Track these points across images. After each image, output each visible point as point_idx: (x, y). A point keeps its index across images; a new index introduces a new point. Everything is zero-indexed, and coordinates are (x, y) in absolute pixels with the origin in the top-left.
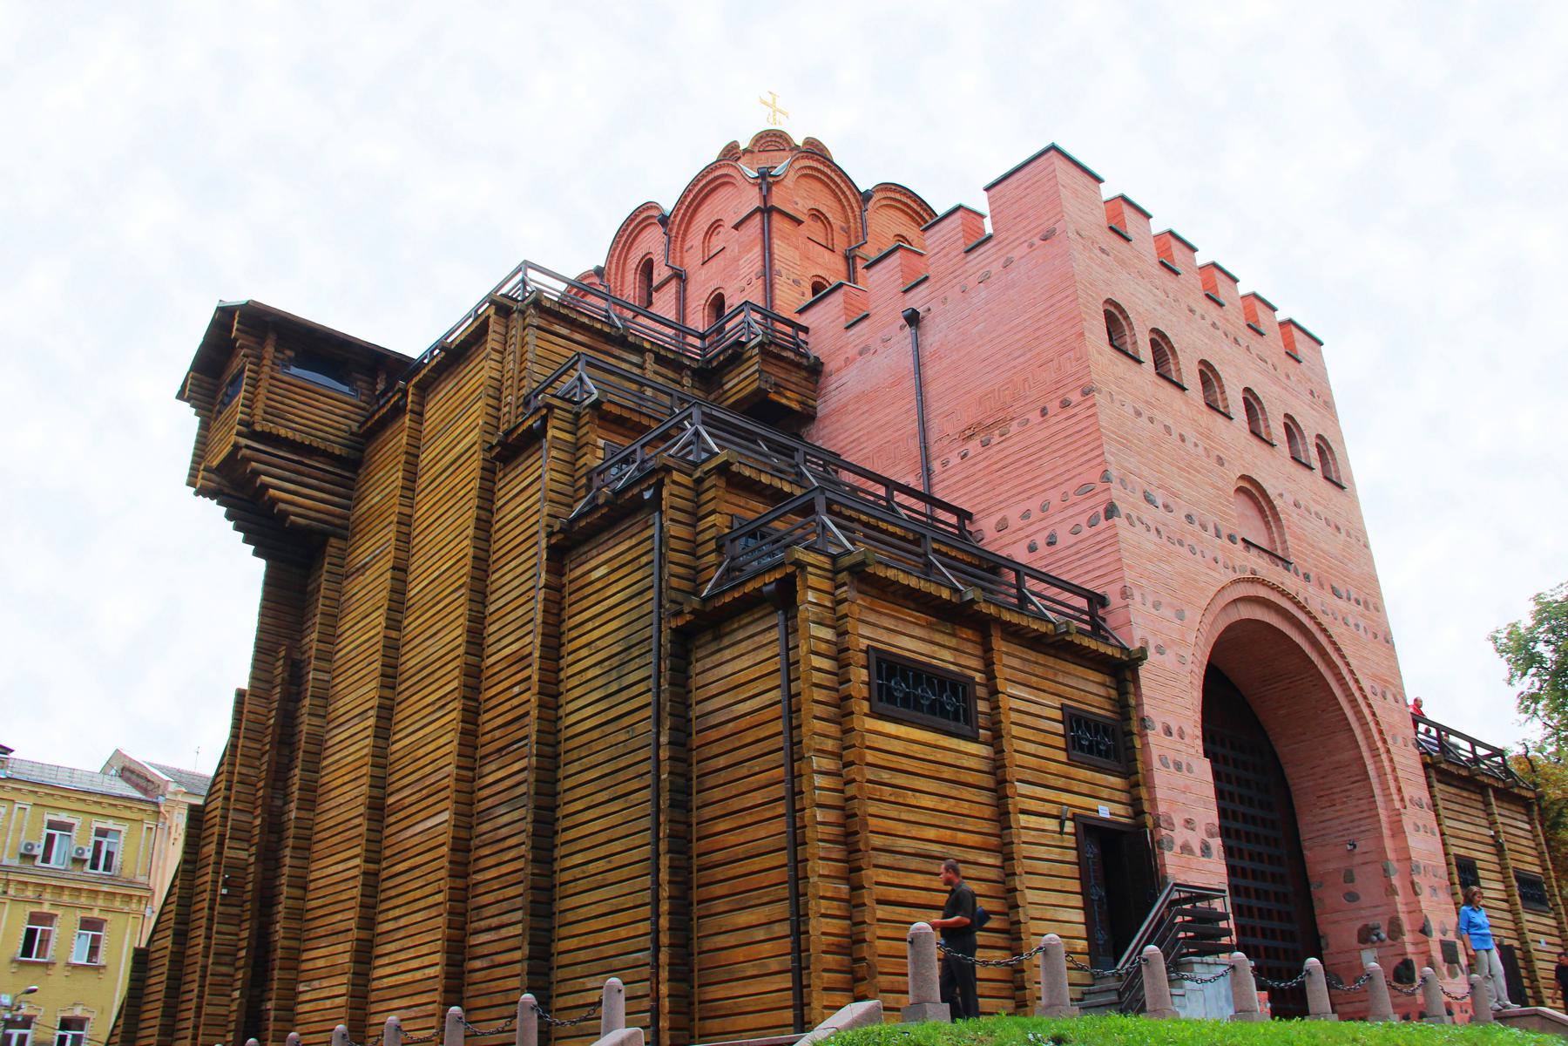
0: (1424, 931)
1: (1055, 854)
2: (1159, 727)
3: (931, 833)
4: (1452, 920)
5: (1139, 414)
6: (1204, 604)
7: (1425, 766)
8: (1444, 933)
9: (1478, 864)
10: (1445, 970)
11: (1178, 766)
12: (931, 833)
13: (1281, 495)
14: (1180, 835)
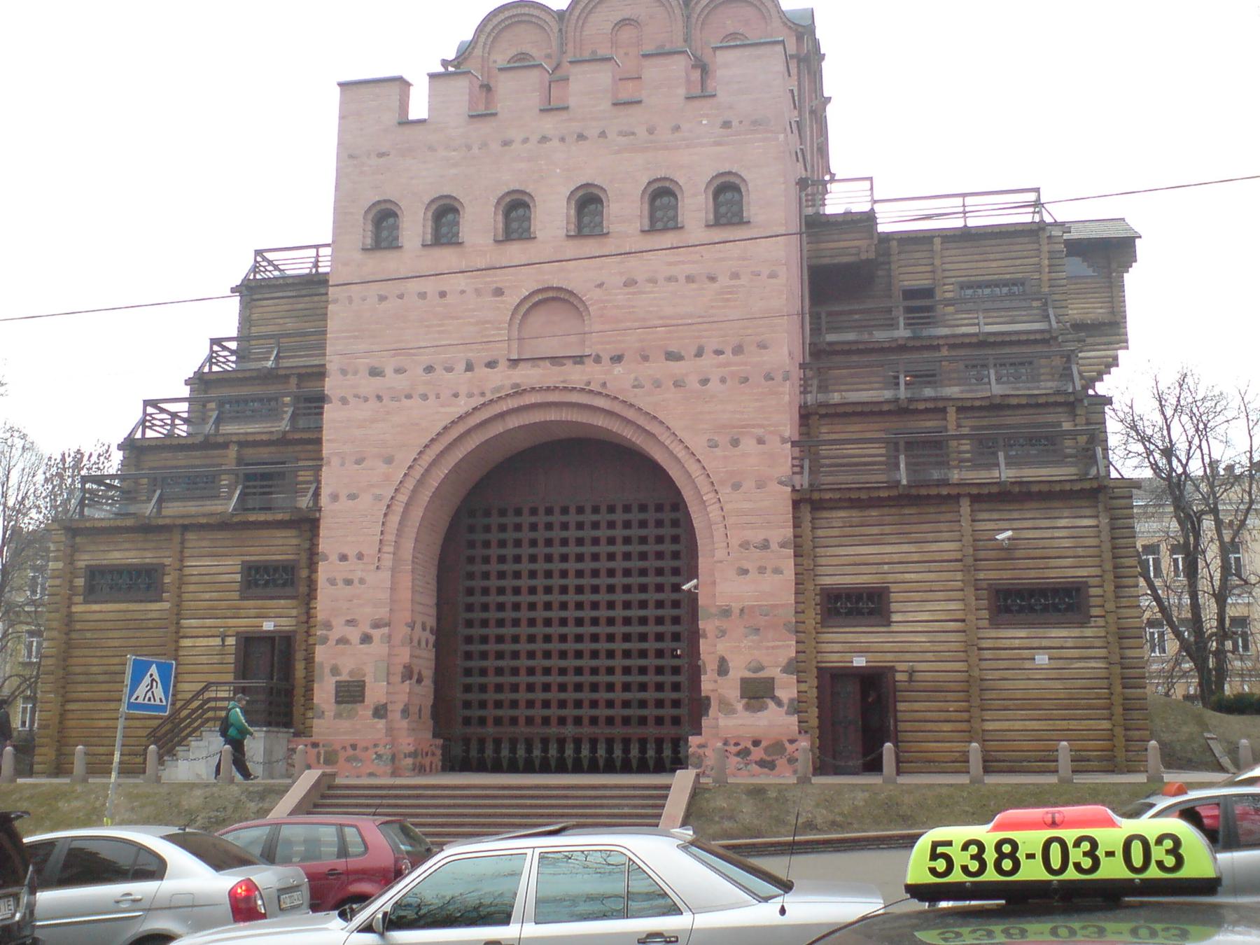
0: (723, 669)
1: (216, 659)
2: (334, 558)
6: (426, 441)
7: (796, 504)
8: (761, 668)
9: (893, 587)
11: (349, 582)
13: (600, 285)
14: (339, 630)
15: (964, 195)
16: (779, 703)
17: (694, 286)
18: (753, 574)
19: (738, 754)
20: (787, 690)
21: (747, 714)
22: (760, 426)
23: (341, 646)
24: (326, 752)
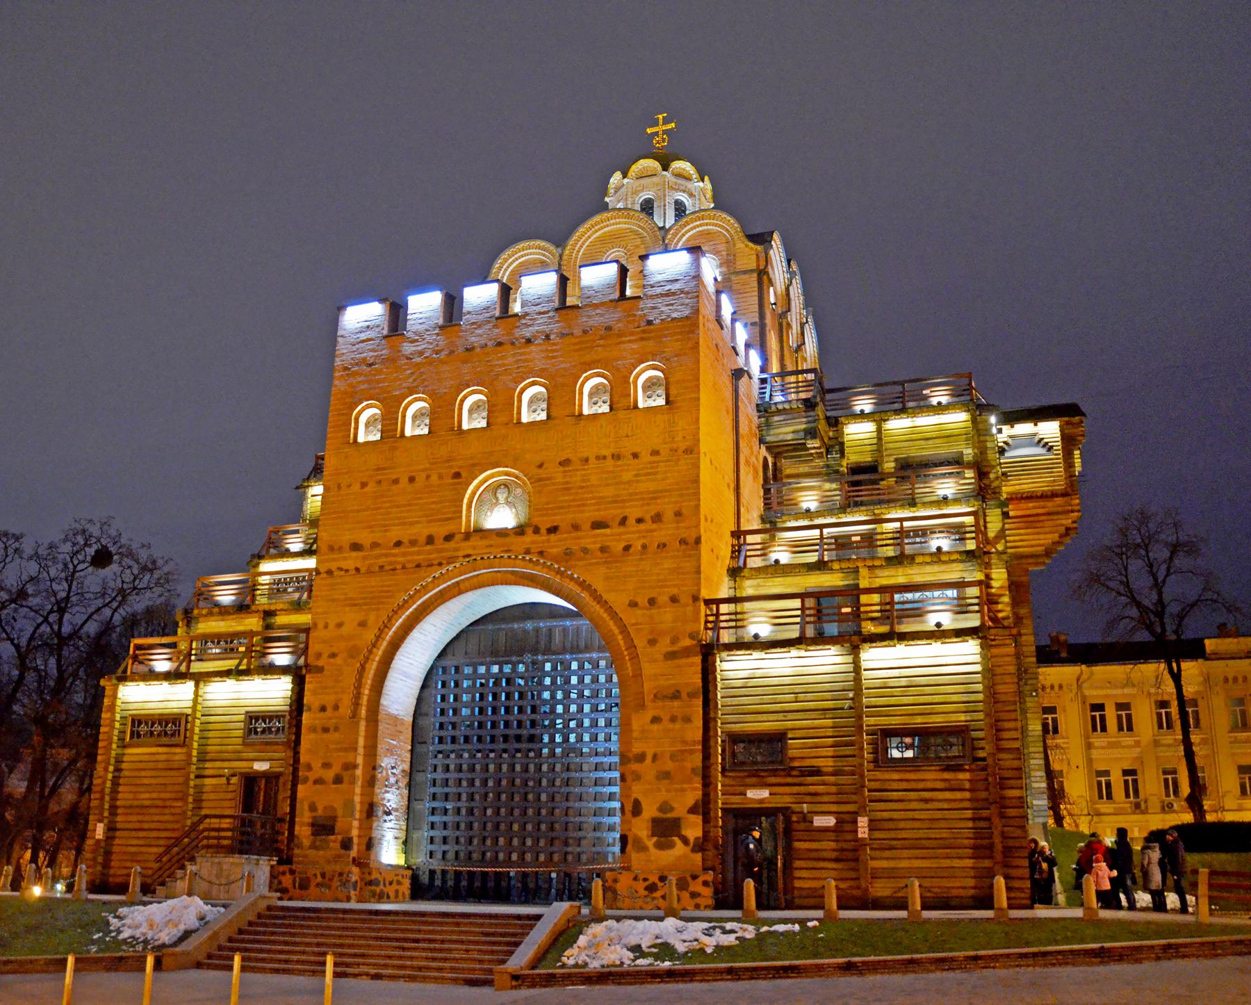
2: (316, 705)
3: (147, 796)
4: (693, 794)
5: (364, 485)
10: (650, 843)
12: (147, 796)
13: (540, 466)
15: (902, 383)
16: (685, 841)
17: (619, 463)
18: (666, 724)
19: (646, 889)
20: (693, 830)
21: (658, 852)
22: (675, 586)
23: (318, 786)
24: (301, 879)
